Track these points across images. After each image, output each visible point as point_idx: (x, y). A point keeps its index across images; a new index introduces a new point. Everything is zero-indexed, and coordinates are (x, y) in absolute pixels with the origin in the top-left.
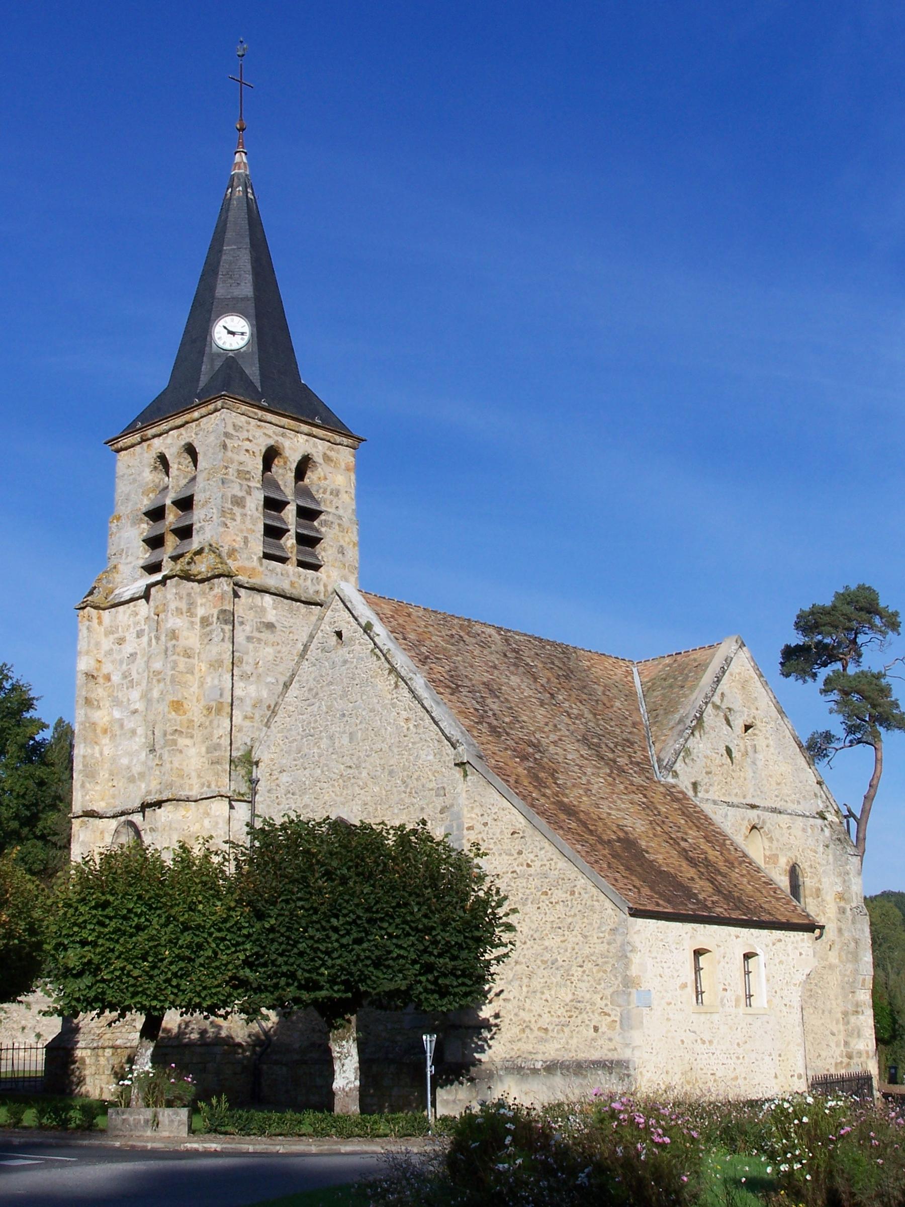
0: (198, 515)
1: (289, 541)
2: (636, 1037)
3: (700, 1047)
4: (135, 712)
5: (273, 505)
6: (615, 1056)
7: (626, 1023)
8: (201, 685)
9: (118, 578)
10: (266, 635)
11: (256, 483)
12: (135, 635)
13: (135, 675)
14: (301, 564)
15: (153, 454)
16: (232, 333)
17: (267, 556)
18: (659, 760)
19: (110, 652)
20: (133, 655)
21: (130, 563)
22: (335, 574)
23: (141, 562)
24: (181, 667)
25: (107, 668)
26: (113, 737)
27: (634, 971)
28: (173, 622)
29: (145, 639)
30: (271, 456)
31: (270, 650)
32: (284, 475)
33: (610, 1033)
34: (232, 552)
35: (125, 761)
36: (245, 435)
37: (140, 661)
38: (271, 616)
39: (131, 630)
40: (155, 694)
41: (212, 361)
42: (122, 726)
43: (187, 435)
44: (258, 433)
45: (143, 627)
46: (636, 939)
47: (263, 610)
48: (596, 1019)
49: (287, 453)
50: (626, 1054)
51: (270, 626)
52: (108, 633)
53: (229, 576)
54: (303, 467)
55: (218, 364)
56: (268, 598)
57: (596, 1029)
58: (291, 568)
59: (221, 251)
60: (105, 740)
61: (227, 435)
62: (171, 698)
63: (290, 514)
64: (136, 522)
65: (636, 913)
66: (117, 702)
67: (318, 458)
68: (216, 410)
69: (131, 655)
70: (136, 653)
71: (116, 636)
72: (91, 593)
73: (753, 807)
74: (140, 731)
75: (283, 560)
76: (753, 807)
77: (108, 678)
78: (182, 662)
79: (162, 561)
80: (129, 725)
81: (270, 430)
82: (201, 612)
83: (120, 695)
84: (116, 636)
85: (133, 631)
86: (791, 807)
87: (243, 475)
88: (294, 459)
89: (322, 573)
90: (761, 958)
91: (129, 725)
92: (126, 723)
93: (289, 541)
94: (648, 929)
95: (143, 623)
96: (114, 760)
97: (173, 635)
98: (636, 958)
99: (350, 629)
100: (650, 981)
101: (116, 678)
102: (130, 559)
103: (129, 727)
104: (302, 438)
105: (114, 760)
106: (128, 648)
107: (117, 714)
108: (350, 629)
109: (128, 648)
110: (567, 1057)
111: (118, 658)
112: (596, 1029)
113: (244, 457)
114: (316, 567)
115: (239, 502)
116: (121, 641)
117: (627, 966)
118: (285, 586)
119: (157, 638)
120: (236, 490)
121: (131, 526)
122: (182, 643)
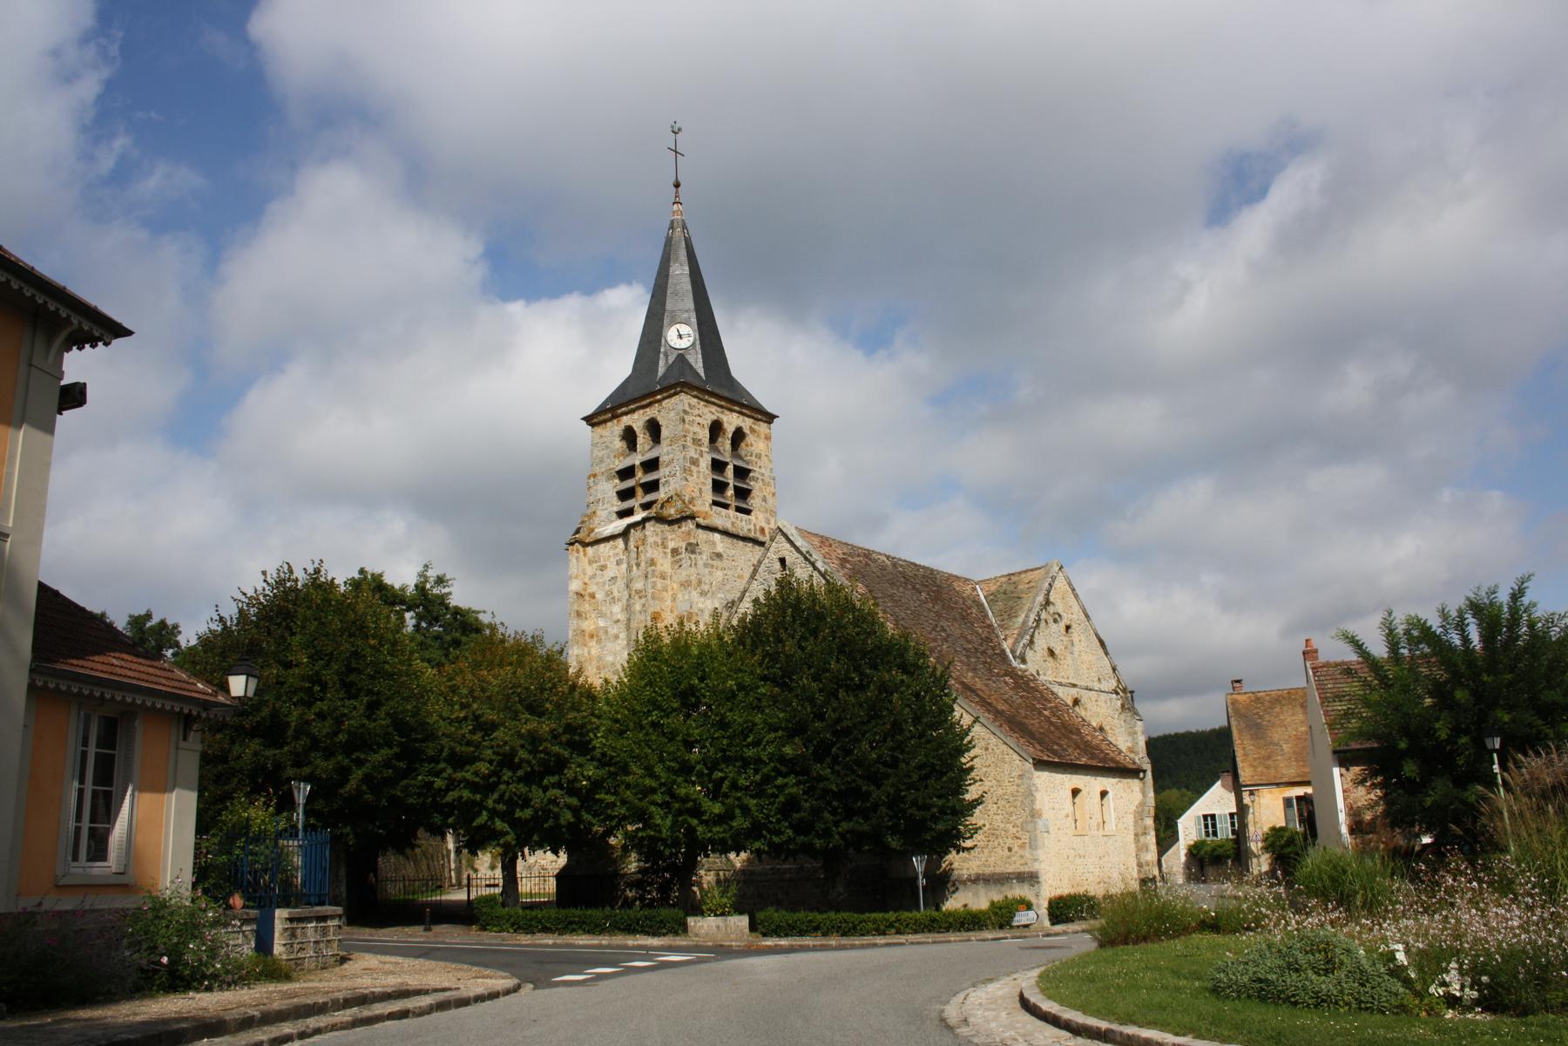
0: (661, 474)
1: (730, 492)
2: (1040, 853)
3: (1078, 861)
5: (718, 466)
6: (1027, 869)
7: (1033, 844)
8: (674, 600)
9: (597, 520)
10: (716, 563)
11: (705, 449)
13: (616, 594)
14: (739, 510)
15: (622, 426)
16: (680, 336)
17: (715, 503)
18: (1013, 652)
19: (594, 576)
20: (614, 579)
22: (761, 516)
23: (616, 509)
24: (659, 586)
25: (592, 588)
26: (599, 641)
27: (1037, 806)
28: (651, 553)
29: (624, 566)
30: (716, 429)
31: (719, 573)
32: (725, 444)
33: (1021, 852)
34: (692, 500)
35: (610, 659)
36: (696, 412)
37: (621, 583)
38: (720, 548)
40: (638, 607)
41: (666, 355)
43: (651, 412)
44: (706, 410)
46: (1037, 781)
47: (714, 543)
48: (1009, 842)
49: (725, 425)
50: (1035, 867)
51: (719, 556)
52: (590, 562)
53: (692, 517)
54: (739, 436)
55: (671, 360)
56: (717, 536)
57: (1010, 849)
58: (731, 512)
59: (667, 276)
60: (593, 643)
61: (685, 412)
62: (651, 610)
63: (730, 470)
64: (610, 478)
65: (1040, 764)
66: (602, 615)
67: (747, 431)
68: (676, 394)
72: (578, 531)
73: (1074, 686)
74: (623, 635)
75: (726, 506)
76: (1074, 686)
77: (593, 596)
78: (660, 583)
80: (613, 630)
81: (714, 409)
82: (671, 545)
85: (613, 560)
86: (1096, 686)
87: (697, 442)
88: (730, 430)
89: (752, 517)
90: (1110, 795)
91: (613, 630)
93: (730, 492)
94: (1043, 778)
96: (600, 658)
97: (652, 562)
98: (1038, 796)
100: (1047, 814)
101: (600, 596)
104: (735, 415)
105: (600, 658)
106: (610, 573)
107: (601, 623)
108: (792, 558)
109: (610, 573)
110: (987, 871)
112: (1010, 849)
113: (696, 429)
114: (748, 512)
115: (695, 462)
116: (603, 568)
117: (1033, 802)
118: (729, 526)
119: (638, 565)
120: (692, 453)
122: (659, 568)
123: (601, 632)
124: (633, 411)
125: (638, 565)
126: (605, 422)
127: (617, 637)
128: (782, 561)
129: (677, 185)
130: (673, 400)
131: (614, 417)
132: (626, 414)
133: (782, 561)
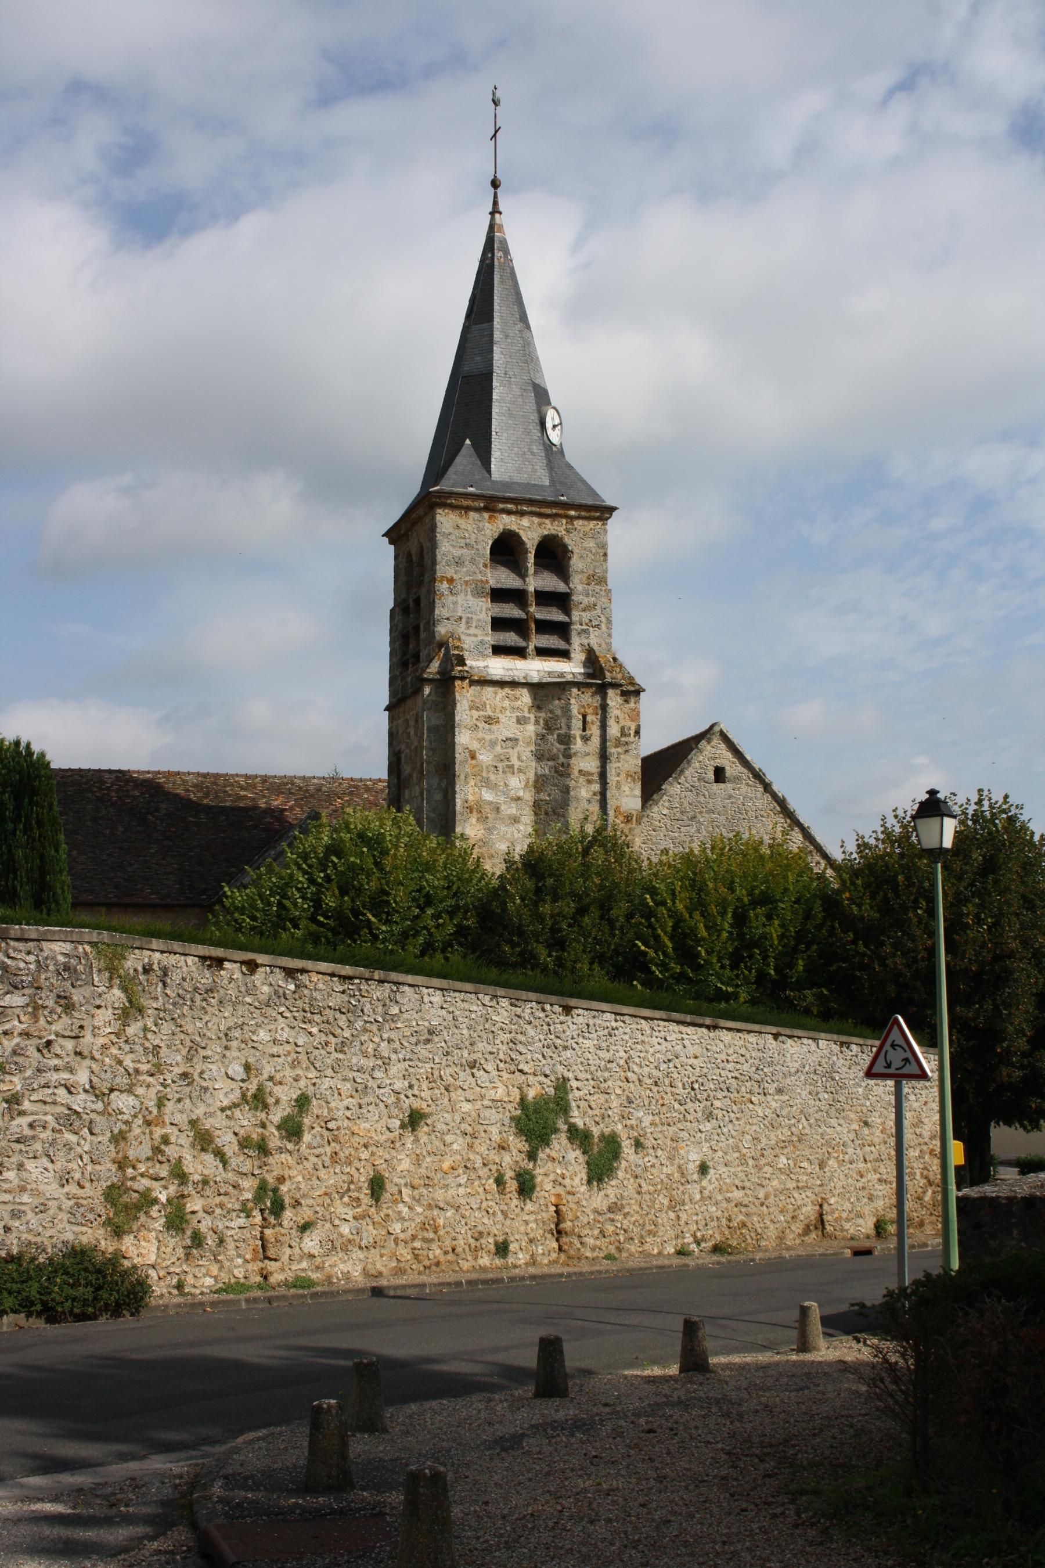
4: (519, 799)
12: (514, 720)
13: (515, 761)
21: (476, 636)
39: (508, 713)
42: (498, 810)
45: (527, 715)
64: (478, 593)
66: (487, 784)
69: (510, 739)
70: (517, 739)
71: (482, 713)
79: (527, 647)
83: (492, 777)
84: (482, 713)
91: (510, 810)
92: (503, 807)
95: (526, 710)
99: (733, 767)
102: (472, 631)
103: (509, 812)
107: (488, 796)
108: (733, 767)
111: (488, 737)
121: (473, 595)
123: (487, 809)
124: (522, 514)
125: (586, 739)
126: (468, 509)
127: (516, 820)
128: (720, 775)
129: (495, 184)
130: (592, 524)
131: (486, 509)
132: (509, 512)
133: (720, 775)
